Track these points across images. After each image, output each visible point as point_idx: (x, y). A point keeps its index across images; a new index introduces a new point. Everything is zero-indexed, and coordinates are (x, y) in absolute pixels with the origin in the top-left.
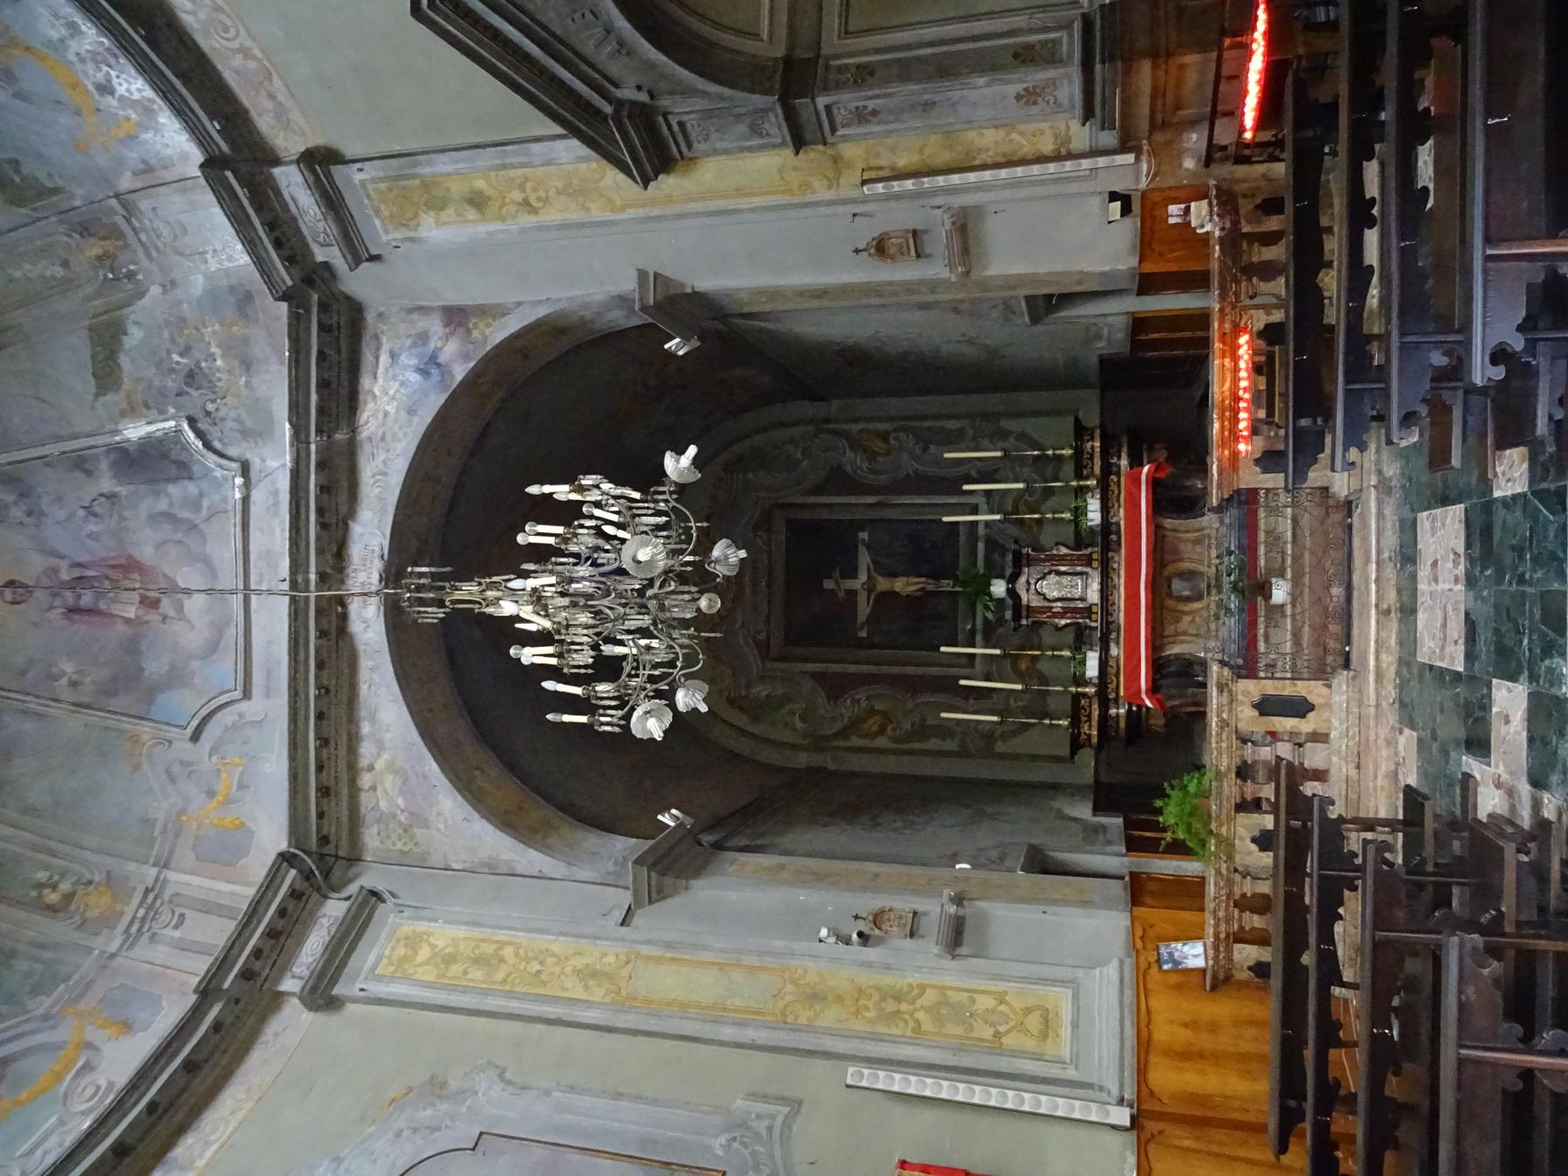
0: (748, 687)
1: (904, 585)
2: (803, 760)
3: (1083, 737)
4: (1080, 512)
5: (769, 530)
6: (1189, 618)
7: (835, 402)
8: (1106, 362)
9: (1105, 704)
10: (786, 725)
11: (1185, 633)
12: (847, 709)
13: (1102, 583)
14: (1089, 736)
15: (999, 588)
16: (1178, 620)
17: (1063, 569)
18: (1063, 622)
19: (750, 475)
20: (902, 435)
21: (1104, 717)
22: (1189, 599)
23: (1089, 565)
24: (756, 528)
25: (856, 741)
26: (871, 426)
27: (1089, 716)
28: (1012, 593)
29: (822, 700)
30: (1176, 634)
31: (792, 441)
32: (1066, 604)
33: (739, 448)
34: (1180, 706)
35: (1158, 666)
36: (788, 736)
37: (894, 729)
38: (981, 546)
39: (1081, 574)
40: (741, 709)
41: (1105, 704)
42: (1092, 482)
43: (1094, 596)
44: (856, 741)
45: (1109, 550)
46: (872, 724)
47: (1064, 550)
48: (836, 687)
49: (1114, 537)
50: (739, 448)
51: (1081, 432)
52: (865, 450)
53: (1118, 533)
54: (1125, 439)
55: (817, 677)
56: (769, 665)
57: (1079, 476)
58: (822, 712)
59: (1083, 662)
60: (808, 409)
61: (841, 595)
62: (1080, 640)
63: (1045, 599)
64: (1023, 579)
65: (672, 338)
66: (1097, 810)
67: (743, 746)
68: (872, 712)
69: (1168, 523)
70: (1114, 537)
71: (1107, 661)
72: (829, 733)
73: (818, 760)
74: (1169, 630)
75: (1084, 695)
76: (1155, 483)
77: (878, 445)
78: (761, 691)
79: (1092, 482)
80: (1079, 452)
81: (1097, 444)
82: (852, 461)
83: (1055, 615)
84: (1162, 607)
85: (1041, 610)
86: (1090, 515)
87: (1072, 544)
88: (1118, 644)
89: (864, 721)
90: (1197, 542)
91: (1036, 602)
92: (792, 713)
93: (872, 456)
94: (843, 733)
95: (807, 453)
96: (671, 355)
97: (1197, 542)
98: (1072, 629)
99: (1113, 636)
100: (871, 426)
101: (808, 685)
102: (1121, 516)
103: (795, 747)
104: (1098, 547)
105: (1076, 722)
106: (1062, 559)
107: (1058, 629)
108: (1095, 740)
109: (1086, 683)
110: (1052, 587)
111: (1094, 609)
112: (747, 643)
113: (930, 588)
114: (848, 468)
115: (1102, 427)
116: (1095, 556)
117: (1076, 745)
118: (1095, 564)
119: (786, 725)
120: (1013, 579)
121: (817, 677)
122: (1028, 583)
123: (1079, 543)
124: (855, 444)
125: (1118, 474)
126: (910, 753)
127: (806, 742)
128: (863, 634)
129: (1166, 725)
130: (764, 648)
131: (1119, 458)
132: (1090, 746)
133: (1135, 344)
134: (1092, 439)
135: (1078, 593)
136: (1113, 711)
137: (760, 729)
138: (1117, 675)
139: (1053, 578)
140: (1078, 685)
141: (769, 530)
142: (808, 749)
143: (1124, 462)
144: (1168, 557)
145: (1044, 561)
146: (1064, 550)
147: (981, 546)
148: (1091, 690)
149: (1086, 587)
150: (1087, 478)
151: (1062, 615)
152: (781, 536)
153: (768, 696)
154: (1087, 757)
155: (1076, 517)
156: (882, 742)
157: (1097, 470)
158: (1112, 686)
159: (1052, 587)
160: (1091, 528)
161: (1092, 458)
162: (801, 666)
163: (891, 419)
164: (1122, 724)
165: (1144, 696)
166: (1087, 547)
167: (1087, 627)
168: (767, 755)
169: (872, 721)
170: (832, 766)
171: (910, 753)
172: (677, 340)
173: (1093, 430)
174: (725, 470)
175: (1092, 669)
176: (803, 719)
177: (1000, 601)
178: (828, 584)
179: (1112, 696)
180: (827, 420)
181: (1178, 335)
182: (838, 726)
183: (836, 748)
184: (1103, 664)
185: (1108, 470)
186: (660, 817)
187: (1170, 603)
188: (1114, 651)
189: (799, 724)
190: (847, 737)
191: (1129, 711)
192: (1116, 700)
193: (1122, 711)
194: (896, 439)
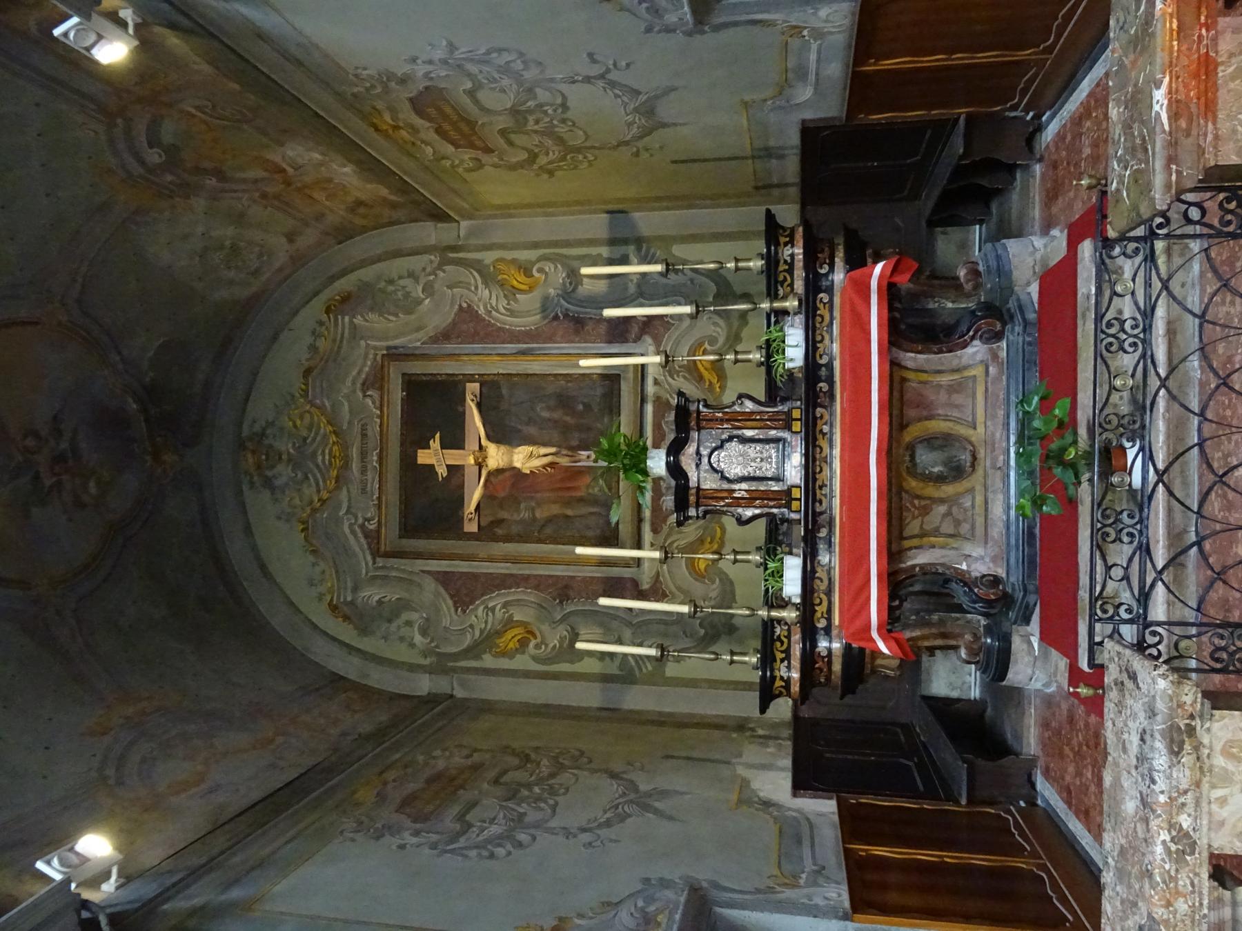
0: (355, 589)
1: (525, 458)
2: (424, 685)
3: (778, 683)
4: (772, 349)
5: (381, 388)
6: (942, 509)
7: (464, 224)
8: (809, 132)
9: (810, 634)
10: (402, 639)
11: (936, 532)
12: (481, 617)
13: (806, 455)
14: (788, 682)
15: (657, 463)
16: (925, 511)
17: (749, 433)
18: (749, 513)
19: (358, 320)
20: (549, 267)
21: (809, 659)
22: (940, 479)
23: (788, 427)
24: (365, 386)
25: (488, 661)
26: (509, 255)
27: (787, 652)
28: (675, 469)
29: (447, 604)
30: (923, 535)
31: (412, 275)
32: (753, 486)
33: (344, 284)
34: (924, 638)
35: (895, 583)
36: (402, 654)
37: (537, 646)
38: (649, 409)
39: (776, 440)
40: (346, 618)
41: (810, 634)
42: (791, 304)
43: (793, 471)
44: (488, 661)
45: (816, 406)
46: (510, 639)
47: (749, 406)
48: (464, 591)
49: (824, 386)
50: (344, 284)
51: (773, 232)
52: (502, 285)
53: (830, 380)
54: (840, 240)
55: (445, 579)
56: (380, 562)
57: (772, 295)
58: (446, 622)
59: (779, 574)
60: (431, 233)
61: (442, 471)
62: (774, 543)
63: (724, 478)
64: (691, 449)
65: (70, 17)
66: (799, 786)
67: (349, 667)
68: (509, 623)
69: (910, 359)
70: (824, 386)
71: (814, 571)
72: (454, 650)
73: (441, 685)
74: (913, 527)
75: (780, 621)
76: (890, 291)
77: (517, 280)
78: (372, 595)
79: (791, 304)
80: (772, 262)
81: (799, 251)
82: (486, 299)
83: (738, 502)
84: (901, 489)
85: (715, 495)
86: (790, 352)
87: (761, 395)
88: (830, 544)
89: (499, 634)
90: (953, 389)
91: (710, 483)
92: (409, 623)
93: (511, 292)
94: (474, 651)
95: (429, 289)
96: (80, 62)
97: (953, 389)
98: (763, 521)
99: (823, 533)
100: (509, 255)
101: (430, 585)
102: (834, 348)
103: (413, 668)
104: (801, 398)
105: (767, 660)
106: (748, 418)
107: (741, 522)
108: (795, 688)
109: (784, 604)
110: (735, 460)
111: (796, 493)
112: (353, 532)
113: (564, 461)
114: (482, 311)
115: (806, 223)
116: (796, 414)
117: (767, 694)
118: (797, 426)
119: (402, 639)
120: (675, 449)
121: (445, 579)
122: (698, 453)
123: (773, 394)
124: (489, 278)
125: (830, 290)
126: (556, 676)
127: (427, 662)
128: (471, 527)
129: (900, 666)
130: (373, 538)
131: (832, 267)
132: (789, 695)
133: (862, 88)
134: (791, 243)
135: (769, 470)
136: (823, 644)
137: (367, 644)
138: (829, 593)
139: (734, 446)
140: (770, 606)
141: (381, 388)
142: (429, 670)
143: (839, 277)
144: (911, 413)
145: (722, 421)
146: (749, 406)
147: (649, 409)
148: (790, 615)
149: (784, 458)
150: (785, 298)
151: (750, 501)
152: (397, 394)
153: (380, 602)
154: (782, 708)
155: (769, 356)
156: (522, 662)
157: (799, 286)
158: (821, 610)
159: (735, 460)
160: (790, 373)
161: (791, 271)
162: (421, 564)
163: (536, 245)
164: (837, 667)
165: (875, 634)
166: (784, 400)
167: (785, 520)
168: (379, 678)
169: (509, 635)
170: (459, 693)
171: (556, 676)
172: (75, 20)
173: (793, 230)
174: (328, 311)
175: (792, 586)
176: (424, 632)
177: (657, 480)
178: (424, 457)
179: (822, 624)
180: (455, 249)
181: (928, 61)
182: (468, 641)
183: (468, 670)
184: (808, 578)
185: (815, 285)
186: (40, 865)
187: (912, 484)
188: (824, 558)
189: (418, 639)
190: (478, 657)
191: (848, 648)
192: (828, 631)
193: (836, 645)
194: (540, 270)
